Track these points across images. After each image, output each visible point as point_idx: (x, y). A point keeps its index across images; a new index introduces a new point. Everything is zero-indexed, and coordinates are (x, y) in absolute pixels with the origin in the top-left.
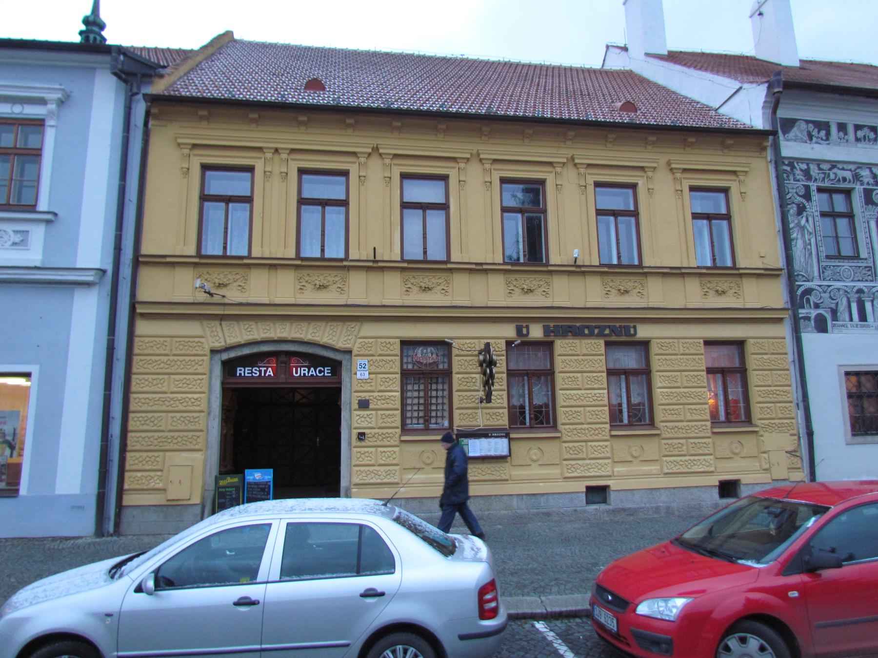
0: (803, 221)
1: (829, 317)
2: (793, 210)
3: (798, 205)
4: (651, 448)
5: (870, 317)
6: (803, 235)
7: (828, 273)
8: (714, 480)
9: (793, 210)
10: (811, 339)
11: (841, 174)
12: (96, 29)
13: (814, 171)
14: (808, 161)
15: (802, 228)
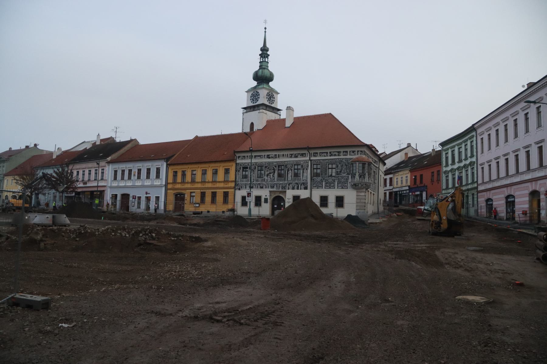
2: (238, 171)
4: (215, 206)
8: (222, 211)
9: (238, 171)
11: (246, 164)
12: (265, 52)
13: (242, 164)
14: (241, 163)
15: (238, 174)
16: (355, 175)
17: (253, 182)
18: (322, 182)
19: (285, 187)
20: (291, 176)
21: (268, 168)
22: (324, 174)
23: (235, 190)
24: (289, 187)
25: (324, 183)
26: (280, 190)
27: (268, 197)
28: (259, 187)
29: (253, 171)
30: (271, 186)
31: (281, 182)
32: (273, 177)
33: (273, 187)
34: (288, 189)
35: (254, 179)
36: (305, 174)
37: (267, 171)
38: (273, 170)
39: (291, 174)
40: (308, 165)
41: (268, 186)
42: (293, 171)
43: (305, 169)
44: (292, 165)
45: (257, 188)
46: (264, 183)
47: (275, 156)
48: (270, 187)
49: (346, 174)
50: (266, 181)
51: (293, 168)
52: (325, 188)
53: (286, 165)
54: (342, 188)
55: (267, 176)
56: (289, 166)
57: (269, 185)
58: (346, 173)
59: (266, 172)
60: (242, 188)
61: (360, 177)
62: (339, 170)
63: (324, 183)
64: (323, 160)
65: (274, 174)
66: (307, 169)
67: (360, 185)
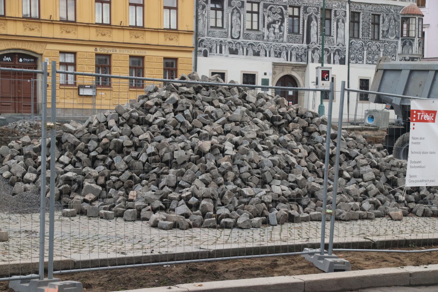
0: (204, 12)
1: (208, 51)
2: (201, 7)
3: (203, 5)
5: (223, 52)
6: (203, 18)
7: (210, 34)
9: (201, 7)
10: (201, 59)
15: (203, 15)
16: (413, 40)
17: (238, 38)
19: (301, 56)
20: (317, 34)
21: (270, 9)
22: (366, 34)
23: (196, 56)
24: (313, 57)
25: (365, 52)
26: (294, 62)
27: (269, 77)
28: (250, 52)
29: (239, 12)
30: (275, 53)
31: (295, 45)
32: (280, 31)
33: (280, 54)
34: (313, 61)
35: (240, 32)
36: (341, 31)
37: (268, 16)
38: (279, 14)
39: (315, 28)
40: (345, 12)
41: (270, 52)
42: (319, 22)
43: (341, 20)
44: (318, 8)
45: (247, 55)
46: (261, 43)
48: (273, 54)
49: (394, 37)
50: (265, 38)
51: (319, 16)
52: (367, 63)
53: (305, 8)
55: (269, 27)
56: (311, 11)
57: (272, 50)
58: (394, 35)
59: (266, 17)
60: (211, 52)
62: (385, 29)
63: (365, 52)
65: (281, 25)
66: (343, 22)
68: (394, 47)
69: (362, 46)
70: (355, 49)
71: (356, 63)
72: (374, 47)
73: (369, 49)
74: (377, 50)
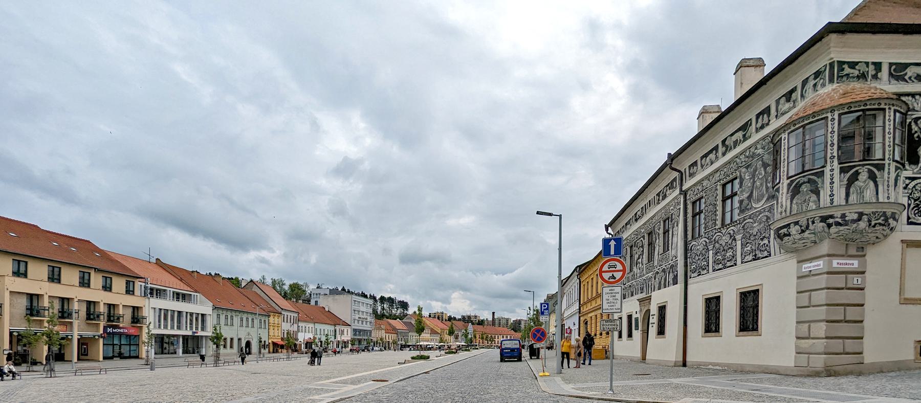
18: (709, 251)
25: (711, 252)
47: (644, 210)
49: (765, 199)
54: (756, 259)
61: (795, 191)
64: (707, 178)
67: (794, 230)
68: (764, 219)
69: (706, 245)
70: (696, 254)
71: (698, 276)
72: (724, 238)
73: (717, 245)
74: (730, 242)
